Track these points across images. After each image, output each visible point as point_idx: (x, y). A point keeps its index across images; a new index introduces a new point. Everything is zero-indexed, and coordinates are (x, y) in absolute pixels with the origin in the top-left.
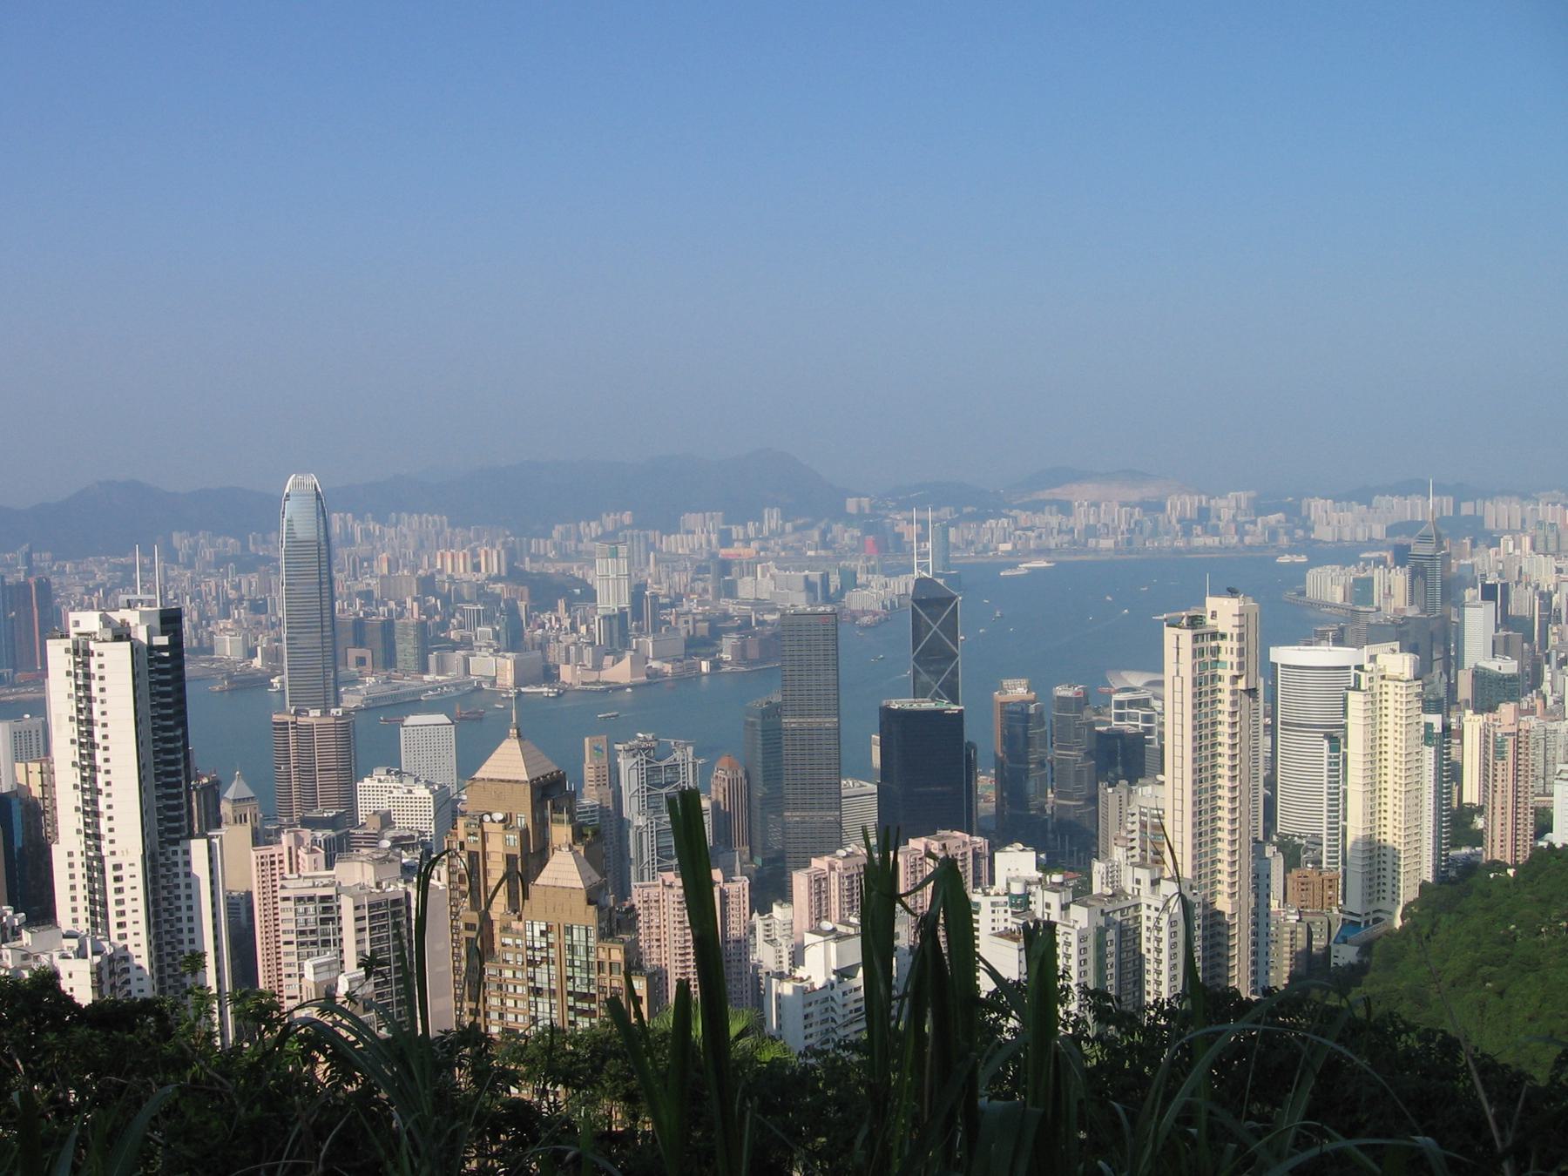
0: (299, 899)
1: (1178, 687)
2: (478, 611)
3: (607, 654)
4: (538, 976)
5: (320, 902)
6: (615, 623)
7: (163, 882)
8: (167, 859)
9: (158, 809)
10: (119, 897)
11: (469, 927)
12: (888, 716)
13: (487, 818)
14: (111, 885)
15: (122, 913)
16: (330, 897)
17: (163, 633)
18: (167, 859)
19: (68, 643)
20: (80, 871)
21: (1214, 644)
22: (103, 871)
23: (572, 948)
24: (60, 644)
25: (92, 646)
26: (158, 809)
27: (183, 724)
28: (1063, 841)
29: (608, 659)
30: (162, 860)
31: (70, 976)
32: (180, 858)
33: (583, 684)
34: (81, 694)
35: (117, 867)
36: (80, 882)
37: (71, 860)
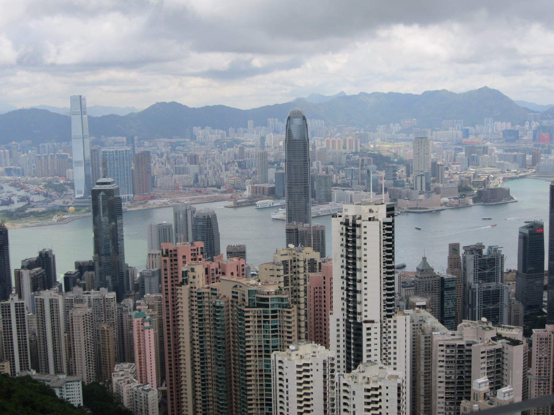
0: (448, 346)
2: (352, 170)
3: (420, 194)
5: (458, 348)
7: (384, 335)
8: (387, 324)
9: (384, 300)
10: (369, 343)
14: (365, 337)
15: (370, 351)
16: (463, 345)
18: (387, 324)
19: (342, 219)
20: (342, 328)
22: (361, 330)
24: (337, 220)
25: (358, 222)
26: (384, 300)
27: (393, 259)
29: (422, 197)
30: (384, 325)
31: (387, 388)
32: (392, 324)
33: (410, 209)
34: (349, 245)
35: (368, 329)
36: (342, 333)
37: (338, 323)
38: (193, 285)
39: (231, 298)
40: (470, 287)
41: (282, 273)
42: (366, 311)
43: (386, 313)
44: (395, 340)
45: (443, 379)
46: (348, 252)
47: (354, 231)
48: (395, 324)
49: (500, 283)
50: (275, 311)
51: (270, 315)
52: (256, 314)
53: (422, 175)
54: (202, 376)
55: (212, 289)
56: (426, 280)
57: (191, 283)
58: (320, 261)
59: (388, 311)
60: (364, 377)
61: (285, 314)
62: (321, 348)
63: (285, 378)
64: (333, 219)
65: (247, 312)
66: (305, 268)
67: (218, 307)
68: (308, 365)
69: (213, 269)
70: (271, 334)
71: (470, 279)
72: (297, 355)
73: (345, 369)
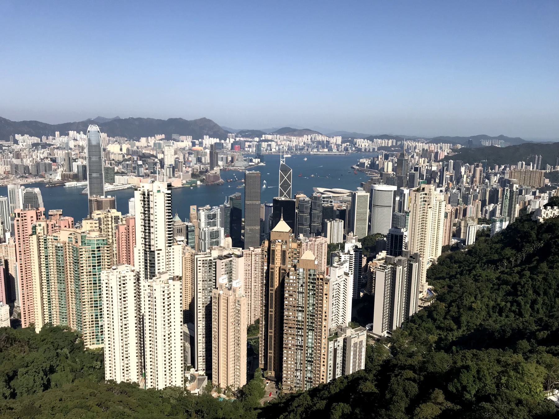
0: (203, 261)
1: (415, 206)
4: (300, 282)
6: (171, 169)
7: (167, 257)
11: (272, 269)
12: (275, 202)
13: (277, 241)
14: (156, 259)
17: (168, 189)
20: (142, 254)
21: (424, 196)
22: (154, 255)
23: (310, 275)
25: (151, 193)
28: (313, 234)
32: (171, 251)
35: (158, 254)
38: (39, 235)
39: (67, 242)
40: (203, 230)
41: (97, 225)
42: (157, 244)
43: (168, 245)
44: (173, 259)
45: (201, 279)
46: (145, 211)
47: (148, 198)
48: (173, 250)
49: (219, 227)
50: (99, 247)
51: (96, 249)
52: (87, 250)
53: (170, 168)
54: (48, 291)
55: (54, 236)
56: (178, 226)
57: (39, 233)
58: (122, 217)
59: (169, 243)
60: (160, 281)
61: (106, 248)
62: (131, 267)
63: (110, 286)
64: (135, 191)
65: (82, 249)
66: (112, 222)
67: (59, 247)
68: (124, 277)
69: (52, 225)
70: (97, 261)
71: (203, 225)
72: (117, 272)
73: (144, 278)
